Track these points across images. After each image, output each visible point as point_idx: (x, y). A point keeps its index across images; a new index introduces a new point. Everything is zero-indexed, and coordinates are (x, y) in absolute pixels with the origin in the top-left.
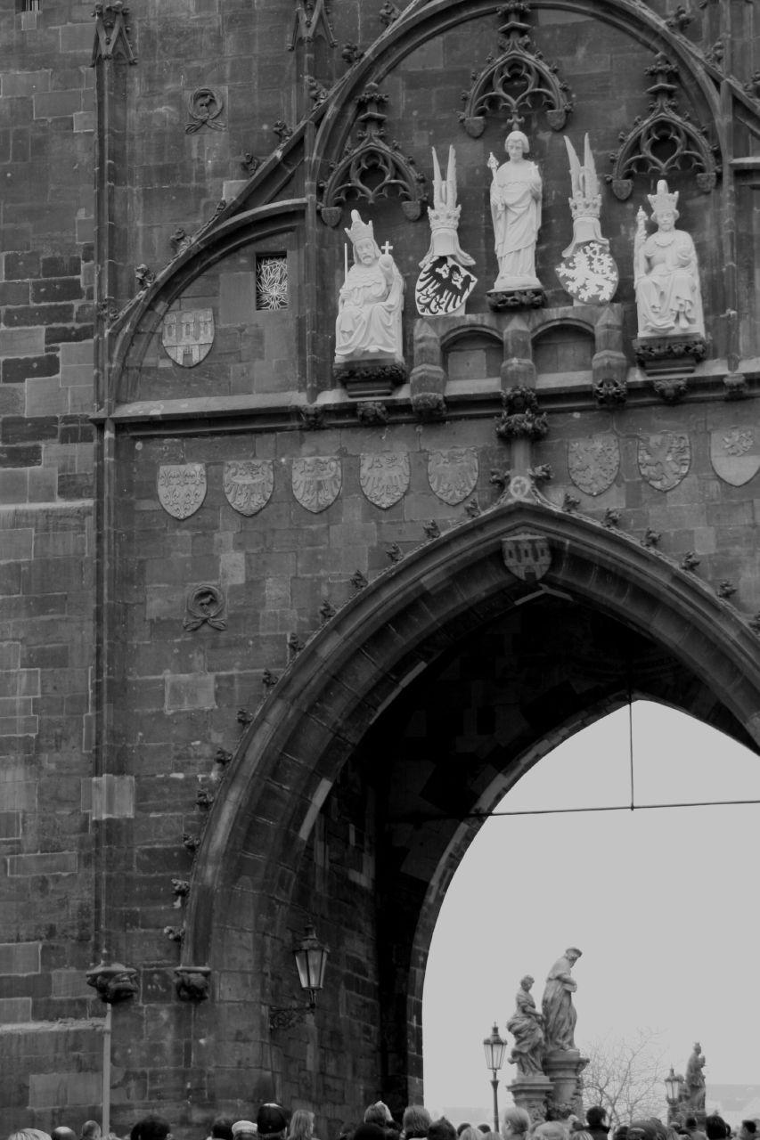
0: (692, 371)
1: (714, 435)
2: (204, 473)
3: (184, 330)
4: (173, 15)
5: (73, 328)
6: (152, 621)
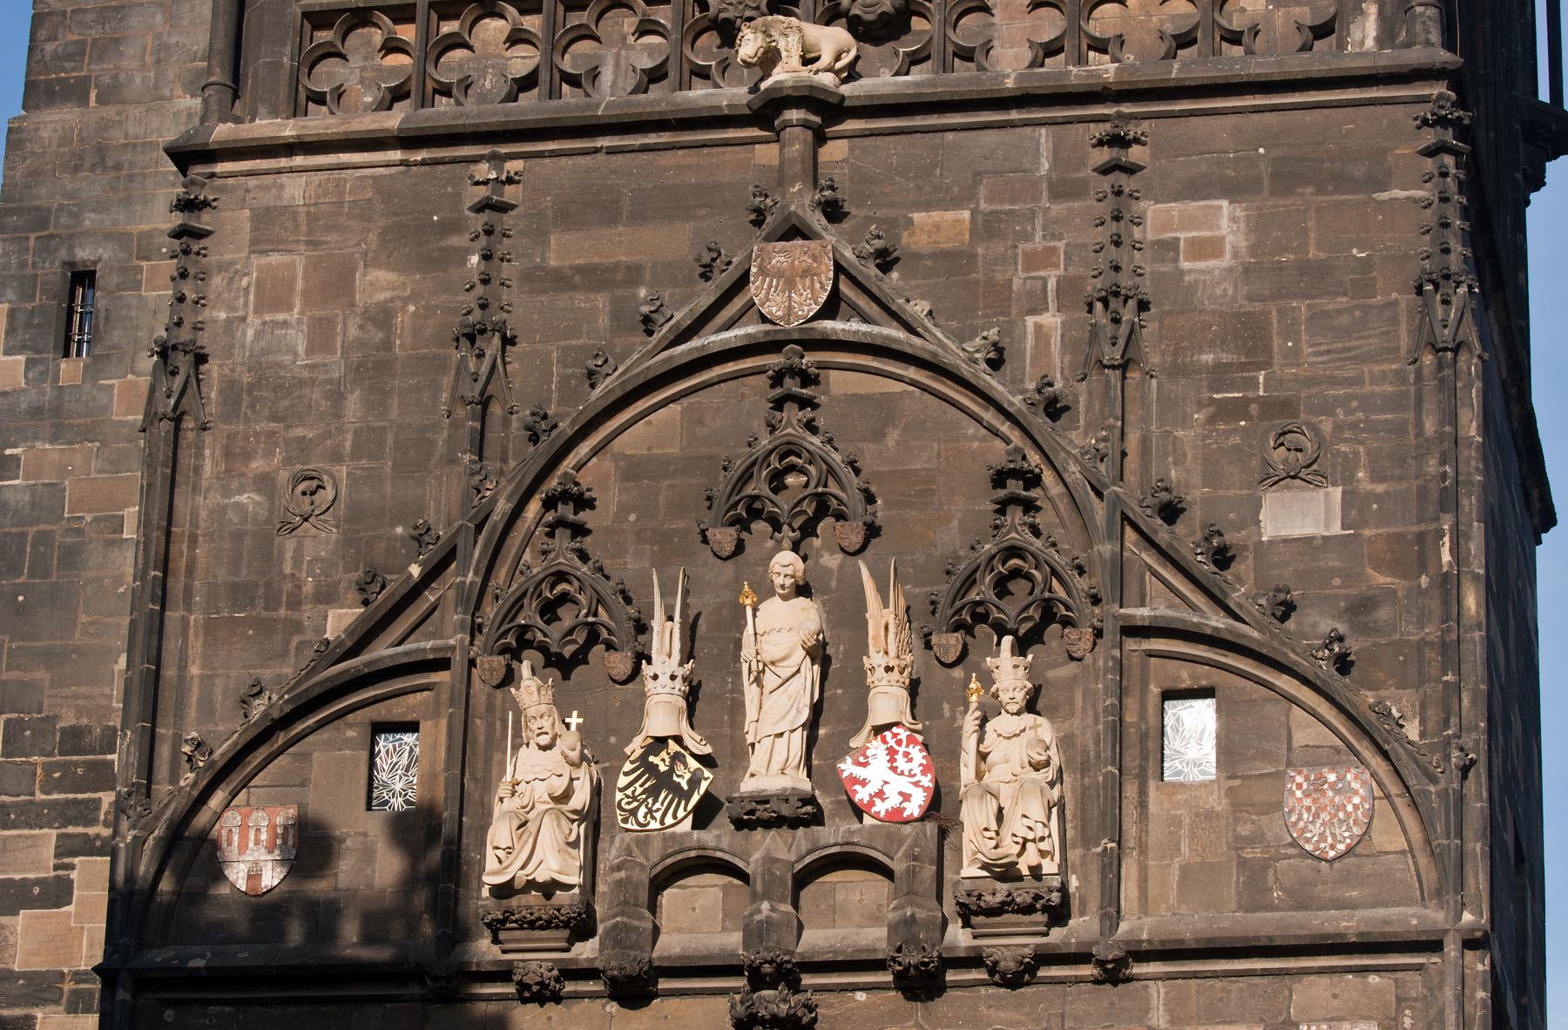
0: (1046, 934)
3: (252, 837)
4: (271, 358)
5: (98, 836)
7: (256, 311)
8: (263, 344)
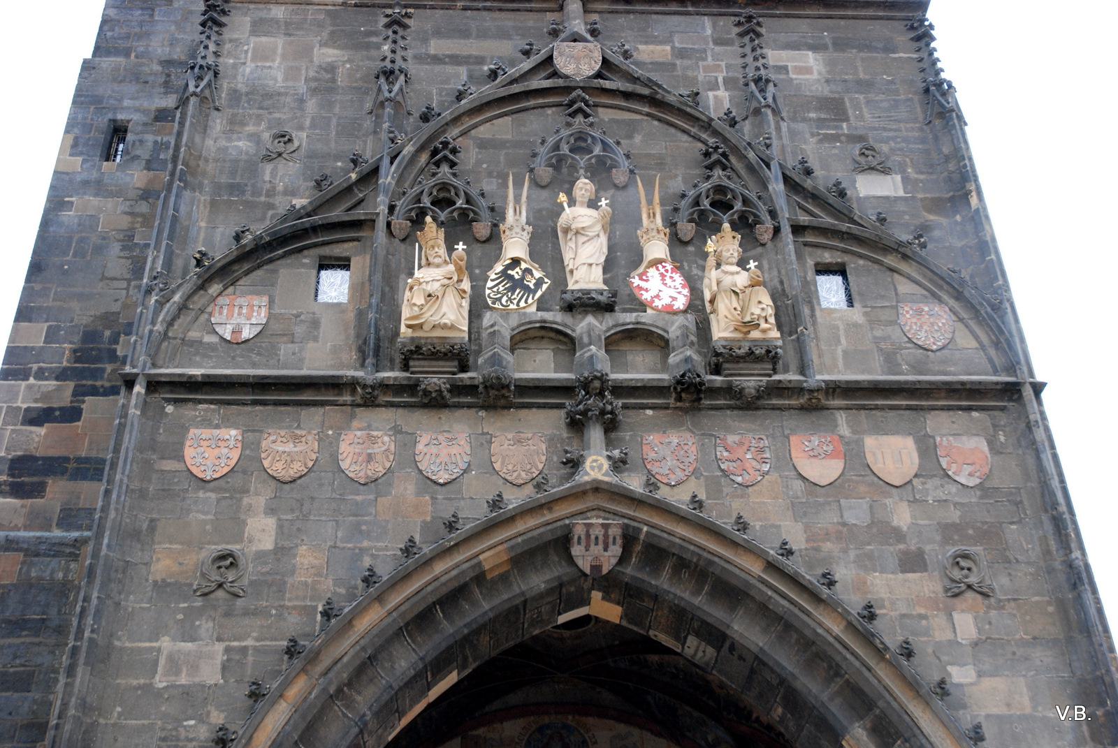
0: (770, 376)
1: (793, 439)
2: (240, 438)
6: (155, 582)
7: (252, 60)
8: (255, 75)
